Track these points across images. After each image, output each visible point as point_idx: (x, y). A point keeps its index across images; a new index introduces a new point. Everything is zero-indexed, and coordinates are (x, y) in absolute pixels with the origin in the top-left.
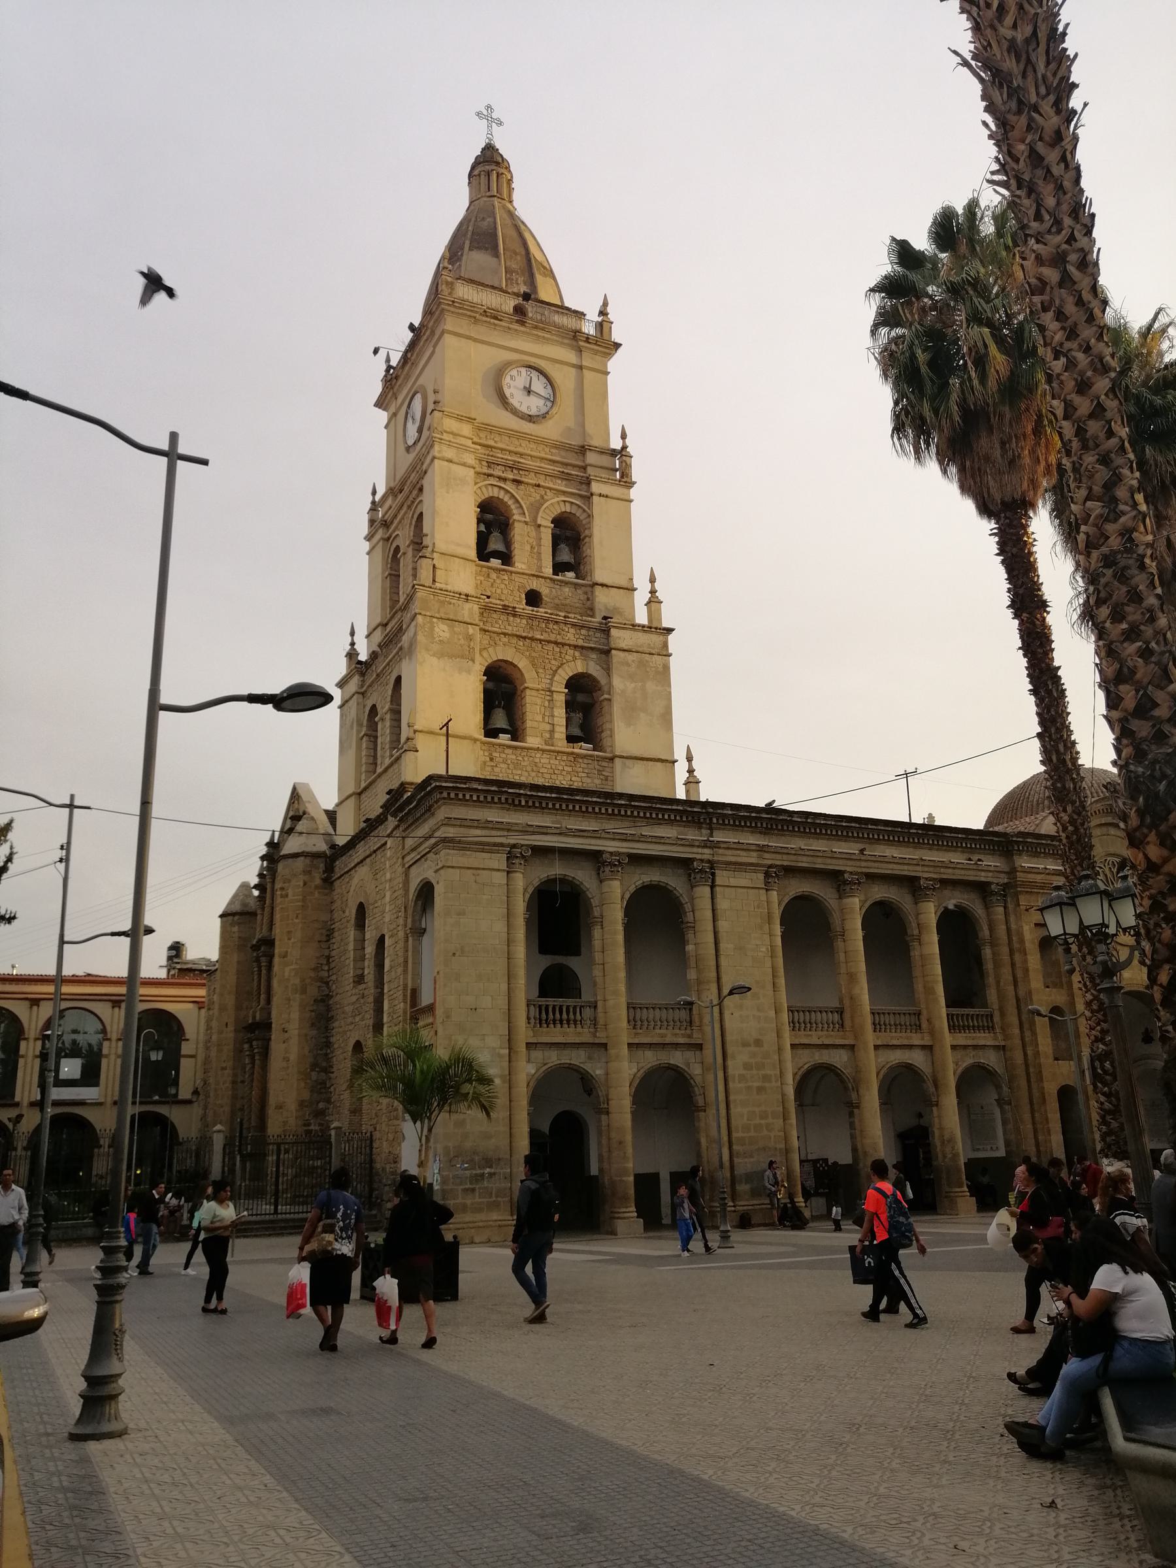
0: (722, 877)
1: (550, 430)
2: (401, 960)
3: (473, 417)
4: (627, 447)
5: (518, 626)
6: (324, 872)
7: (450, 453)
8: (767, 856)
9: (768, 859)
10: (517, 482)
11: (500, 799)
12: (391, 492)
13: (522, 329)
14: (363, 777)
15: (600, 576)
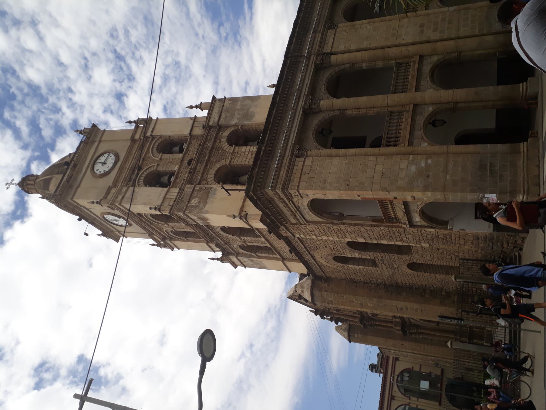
0: (327, 49)
1: (122, 157)
2: (356, 228)
3: (108, 187)
4: (135, 121)
5: (201, 168)
6: (322, 281)
7: (120, 197)
8: (319, 29)
9: (321, 28)
10: (140, 169)
11: (266, 160)
12: (151, 236)
13: (78, 166)
14: (275, 256)
15: (187, 132)
